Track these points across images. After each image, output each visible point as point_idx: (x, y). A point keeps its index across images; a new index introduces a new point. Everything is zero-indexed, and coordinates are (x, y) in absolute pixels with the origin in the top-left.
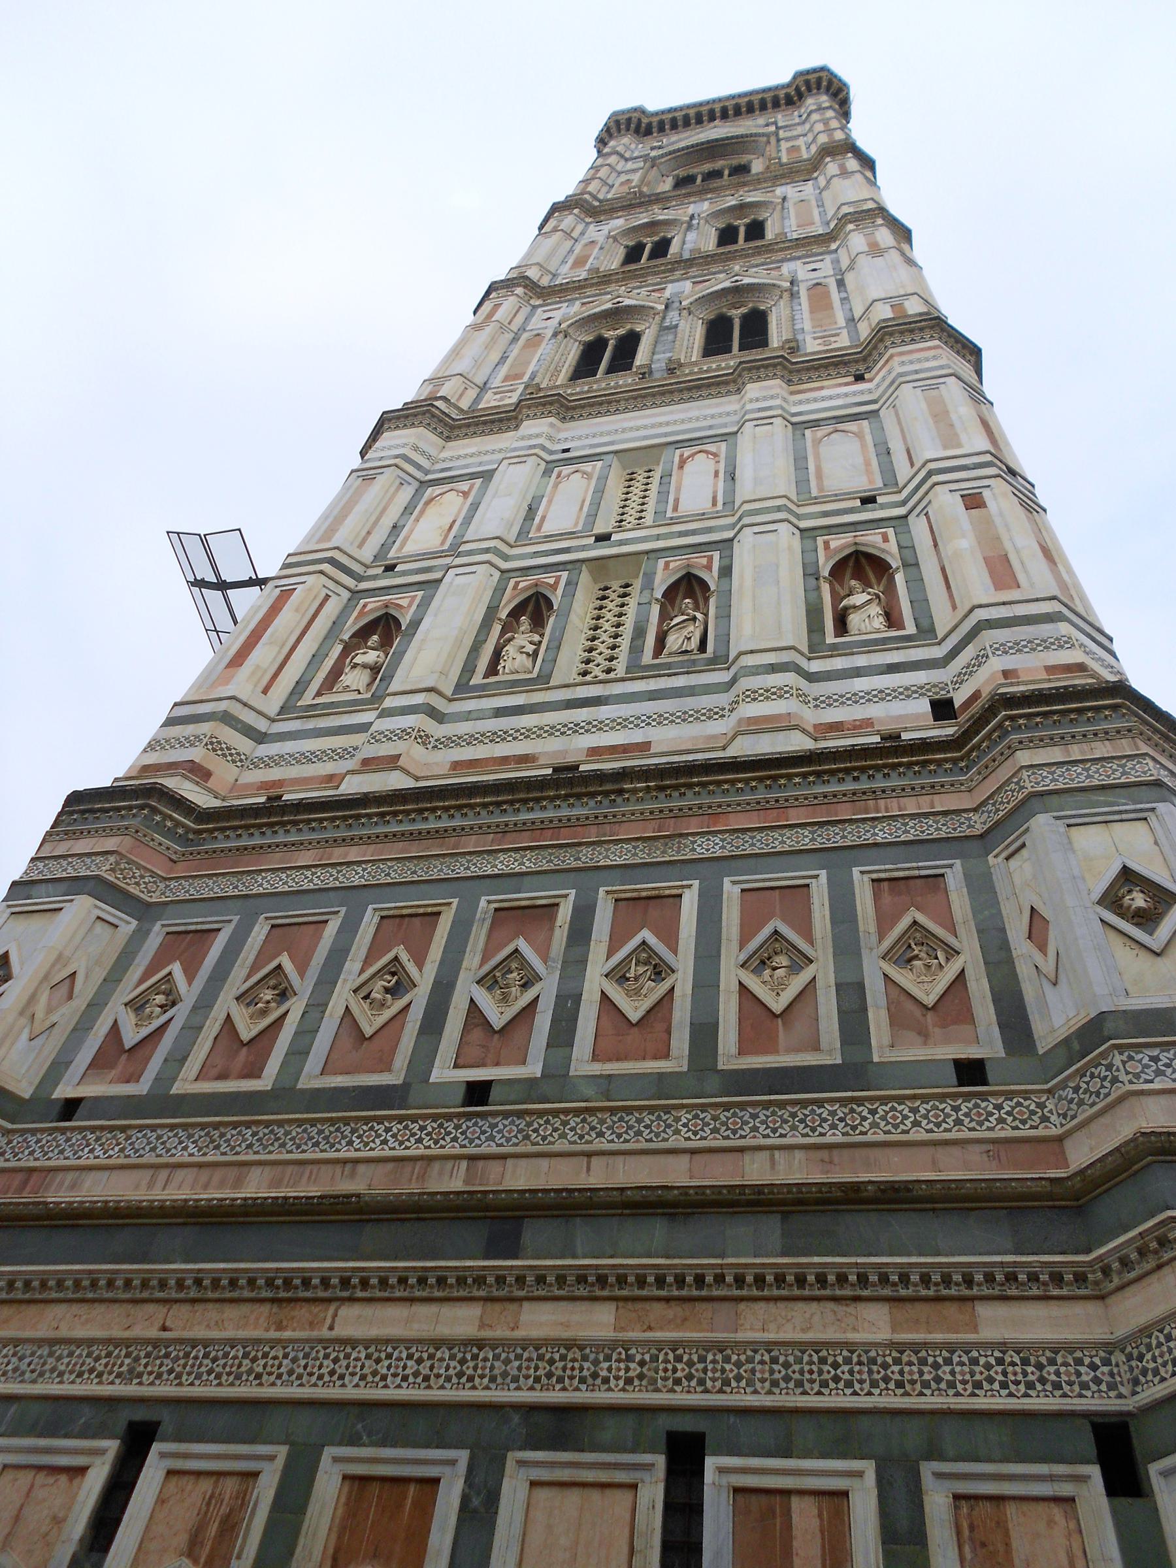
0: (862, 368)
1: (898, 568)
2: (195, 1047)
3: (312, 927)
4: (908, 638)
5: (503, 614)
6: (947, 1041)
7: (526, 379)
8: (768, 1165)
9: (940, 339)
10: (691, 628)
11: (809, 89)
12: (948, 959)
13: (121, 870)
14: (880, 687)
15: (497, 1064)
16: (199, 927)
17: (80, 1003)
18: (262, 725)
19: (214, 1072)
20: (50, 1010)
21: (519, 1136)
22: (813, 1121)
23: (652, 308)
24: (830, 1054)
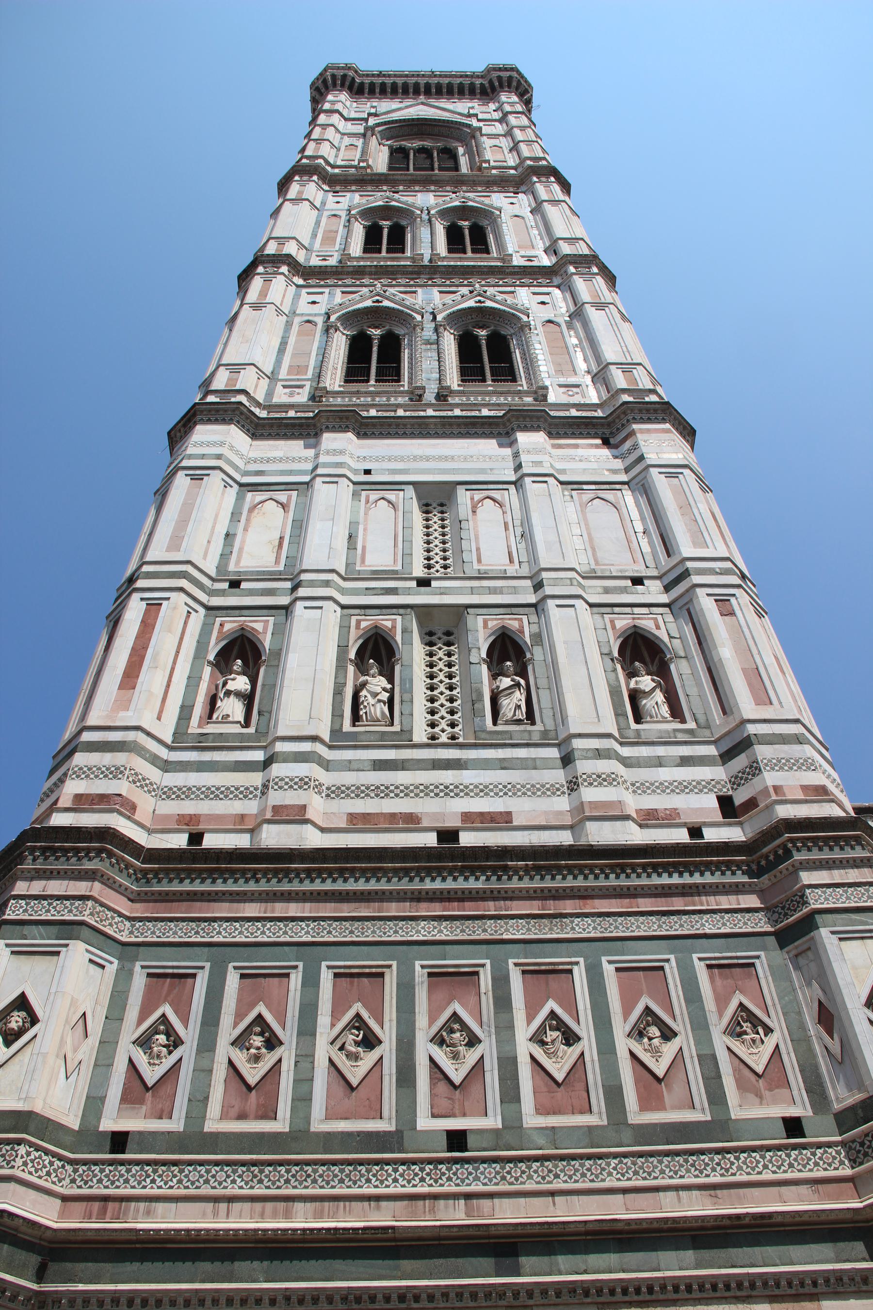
0: (607, 431)
1: (671, 659)
2: (212, 1089)
3: (276, 980)
4: (690, 732)
5: (352, 655)
6: (775, 1102)
7: (310, 374)
8: (676, 1200)
9: (670, 422)
11: (501, 86)
12: (766, 1035)
13: (98, 913)
14: (679, 779)
15: (464, 1115)
16: (176, 971)
17: (94, 1040)
18: (164, 753)
19: (234, 1112)
20: (75, 1050)
21: (498, 1177)
22: (700, 1165)
23: (411, 316)
24: (700, 1115)
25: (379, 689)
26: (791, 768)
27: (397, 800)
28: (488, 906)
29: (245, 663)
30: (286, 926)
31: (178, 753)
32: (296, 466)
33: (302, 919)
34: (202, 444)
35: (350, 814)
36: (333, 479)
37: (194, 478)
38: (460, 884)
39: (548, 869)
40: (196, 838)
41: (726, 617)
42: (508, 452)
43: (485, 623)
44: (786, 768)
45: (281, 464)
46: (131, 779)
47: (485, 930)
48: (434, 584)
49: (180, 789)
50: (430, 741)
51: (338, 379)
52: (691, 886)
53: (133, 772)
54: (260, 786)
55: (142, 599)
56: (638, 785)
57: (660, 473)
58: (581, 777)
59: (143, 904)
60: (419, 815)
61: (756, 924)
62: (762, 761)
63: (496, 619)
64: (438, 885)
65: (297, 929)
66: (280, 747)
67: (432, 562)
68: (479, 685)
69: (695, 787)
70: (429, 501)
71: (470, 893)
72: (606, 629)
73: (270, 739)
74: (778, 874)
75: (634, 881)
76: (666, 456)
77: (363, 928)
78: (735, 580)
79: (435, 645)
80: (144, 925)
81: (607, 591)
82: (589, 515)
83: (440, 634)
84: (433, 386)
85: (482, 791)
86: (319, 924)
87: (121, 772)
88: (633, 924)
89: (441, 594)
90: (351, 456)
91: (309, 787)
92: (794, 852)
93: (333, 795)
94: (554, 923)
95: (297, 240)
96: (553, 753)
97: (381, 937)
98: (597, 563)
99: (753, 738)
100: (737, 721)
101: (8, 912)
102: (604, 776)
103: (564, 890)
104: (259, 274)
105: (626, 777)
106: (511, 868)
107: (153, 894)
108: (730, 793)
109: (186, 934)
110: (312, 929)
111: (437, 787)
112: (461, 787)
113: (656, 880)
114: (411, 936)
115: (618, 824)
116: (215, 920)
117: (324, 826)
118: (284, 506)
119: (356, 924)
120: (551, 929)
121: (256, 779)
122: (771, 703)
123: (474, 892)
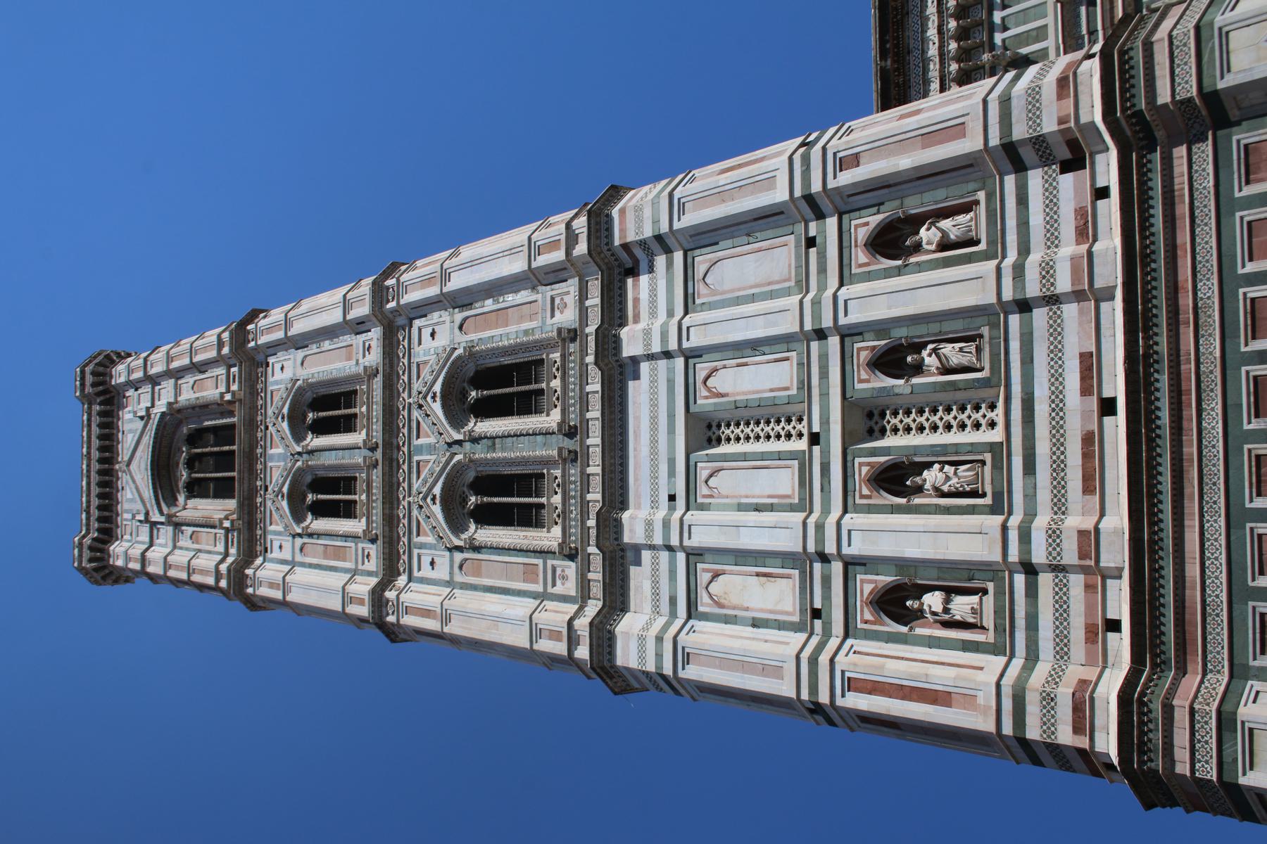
7: (539, 562)
18: (1018, 663)
28: (1185, 370)
31: (1017, 649)
35: (1083, 492)
37: (687, 658)
42: (645, 367)
45: (661, 582)
51: (539, 534)
59: (1188, 665)
63: (859, 371)
66: (1014, 556)
74: (1156, 123)
80: (1210, 661)
84: (554, 440)
86: (1206, 512)
95: (346, 584)
96: (1014, 320)
99: (1004, 141)
101: (1209, 777)
102: (1044, 273)
103: (1169, 306)
104: (398, 620)
115: (1096, 260)
119: (1206, 479)
121: (1045, 580)
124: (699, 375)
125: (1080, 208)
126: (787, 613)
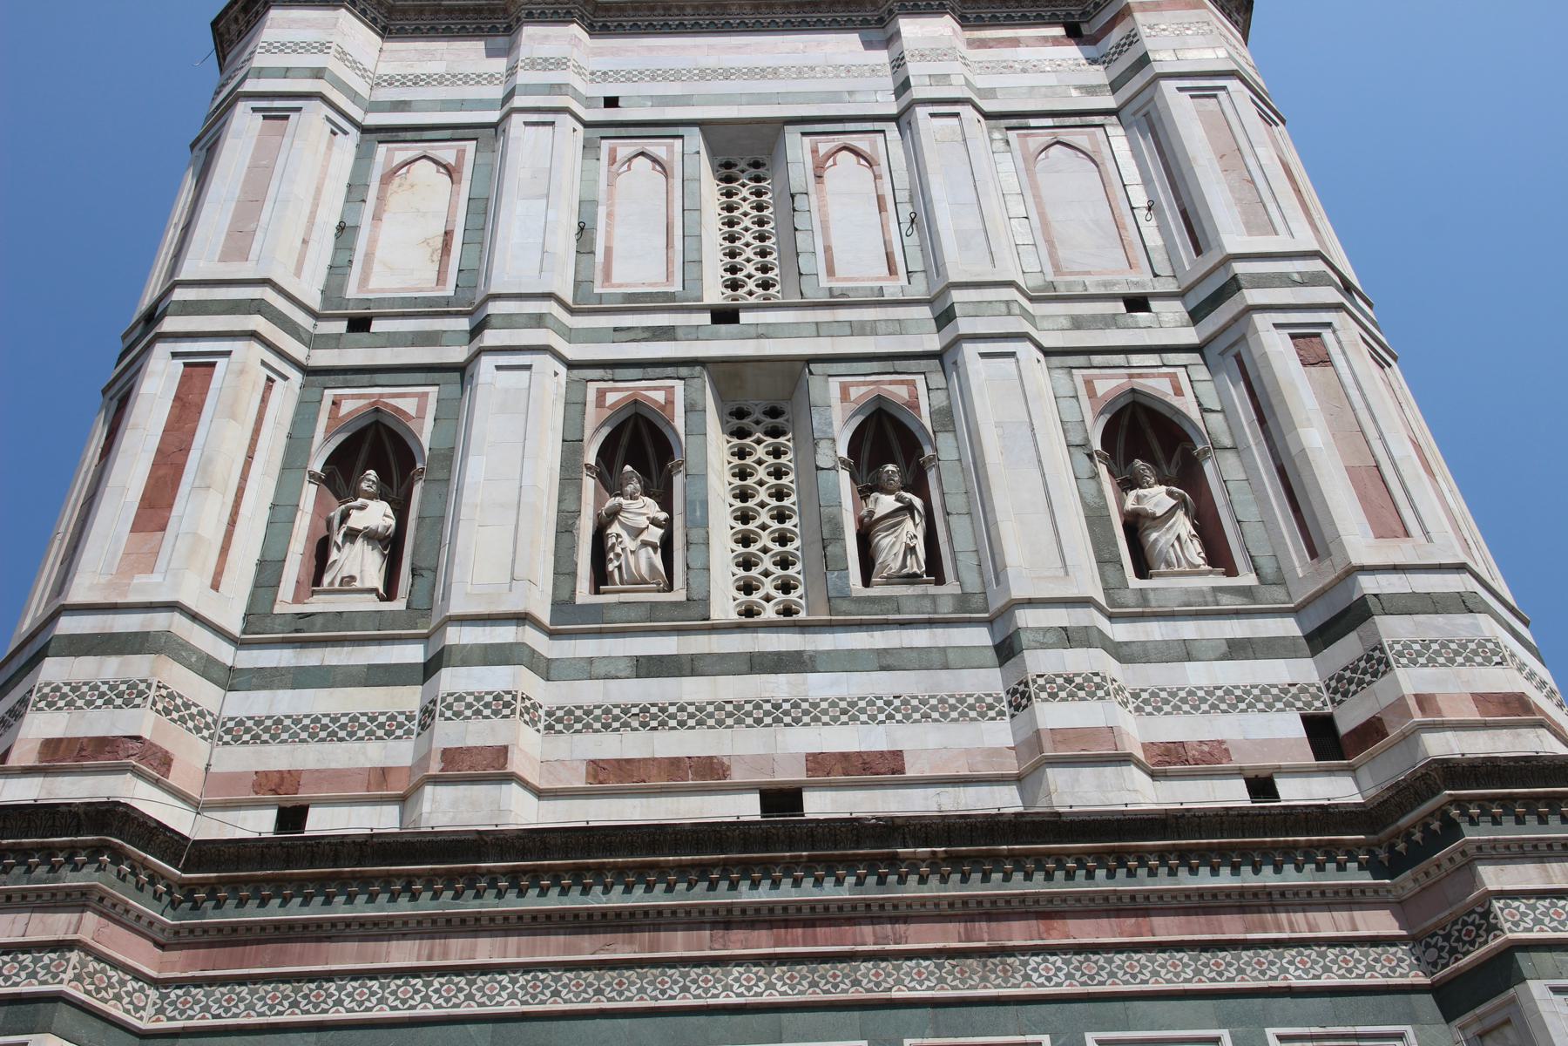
1: (1205, 452)
4: (1246, 592)
5: (591, 457)
10: (909, 524)
13: (91, 975)
18: (225, 654)
25: (643, 522)
26: (1451, 661)
27: (682, 732)
28: (862, 936)
29: (384, 477)
30: (470, 983)
31: (255, 653)
32: (471, 92)
33: (502, 969)
34: (282, 48)
35: (594, 762)
36: (544, 117)
37: (270, 116)
38: (808, 892)
39: (976, 860)
40: (292, 817)
41: (1312, 369)
42: (882, 57)
43: (845, 390)
44: (1441, 660)
45: (441, 88)
46: (160, 706)
47: (856, 983)
48: (745, 317)
49: (258, 723)
50: (744, 619)
52: (1256, 892)
53: (164, 692)
54: (417, 713)
55: (175, 355)
56: (1145, 695)
57: (1180, 89)
58: (1034, 682)
59: (185, 952)
60: (725, 760)
61: (1393, 970)
62: (1391, 648)
64: (764, 895)
65: (492, 989)
66: (456, 636)
67: (740, 275)
68: (835, 510)
69: (1258, 699)
70: (733, 158)
71: (827, 909)
72: (1076, 397)
73: (435, 621)
74: (1433, 870)
75: (1144, 883)
76: (1192, 55)
77: (620, 984)
78: (1332, 295)
79: (749, 434)
80: (187, 993)
81: (1078, 323)
82: (1041, 178)
83: (757, 415)
85: (844, 712)
86: (535, 978)
87: (141, 694)
88: (1146, 967)
89: (759, 337)
90: (579, 70)
91: (513, 712)
92: (1465, 827)
93: (559, 727)
94: (990, 966)
96: (980, 637)
97: (656, 999)
98: (1057, 270)
99: (1372, 602)
100: (1339, 570)
102: (1078, 680)
103: (1008, 902)
105: (1121, 682)
106: (903, 860)
107: (205, 931)
108: (1329, 709)
109: (271, 1008)
110: (522, 987)
111: (758, 706)
112: (805, 705)
113: (1187, 881)
114: (714, 996)
115: (1109, 771)
116: (329, 976)
117: (543, 785)
118: (450, 171)
119: (609, 975)
120: (984, 979)
121: (409, 698)
122: (1407, 534)
123: (833, 908)
124: (860, 140)
125: (1226, 750)
126: (364, 279)
